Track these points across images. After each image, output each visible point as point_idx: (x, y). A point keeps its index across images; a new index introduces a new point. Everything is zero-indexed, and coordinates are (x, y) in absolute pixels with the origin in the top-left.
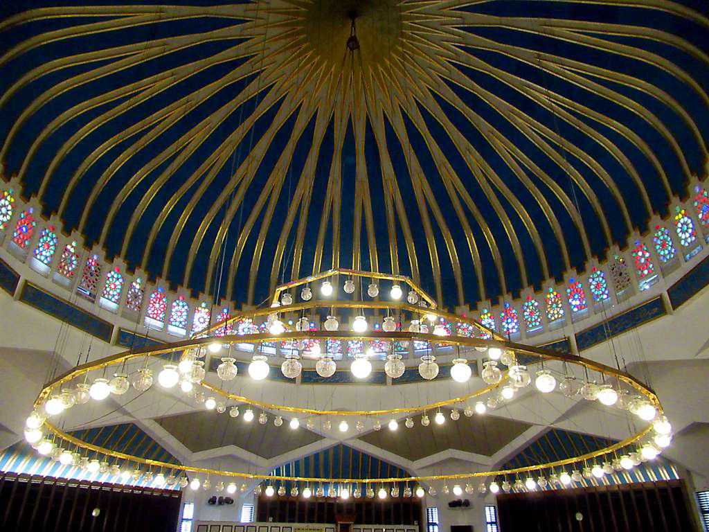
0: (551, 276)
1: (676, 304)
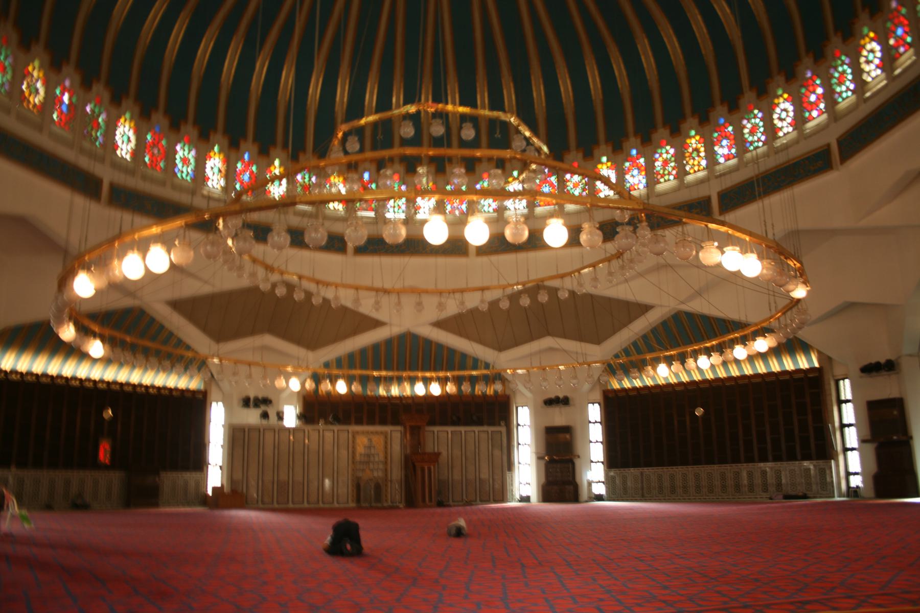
0: (693, 113)
1: (845, 156)
